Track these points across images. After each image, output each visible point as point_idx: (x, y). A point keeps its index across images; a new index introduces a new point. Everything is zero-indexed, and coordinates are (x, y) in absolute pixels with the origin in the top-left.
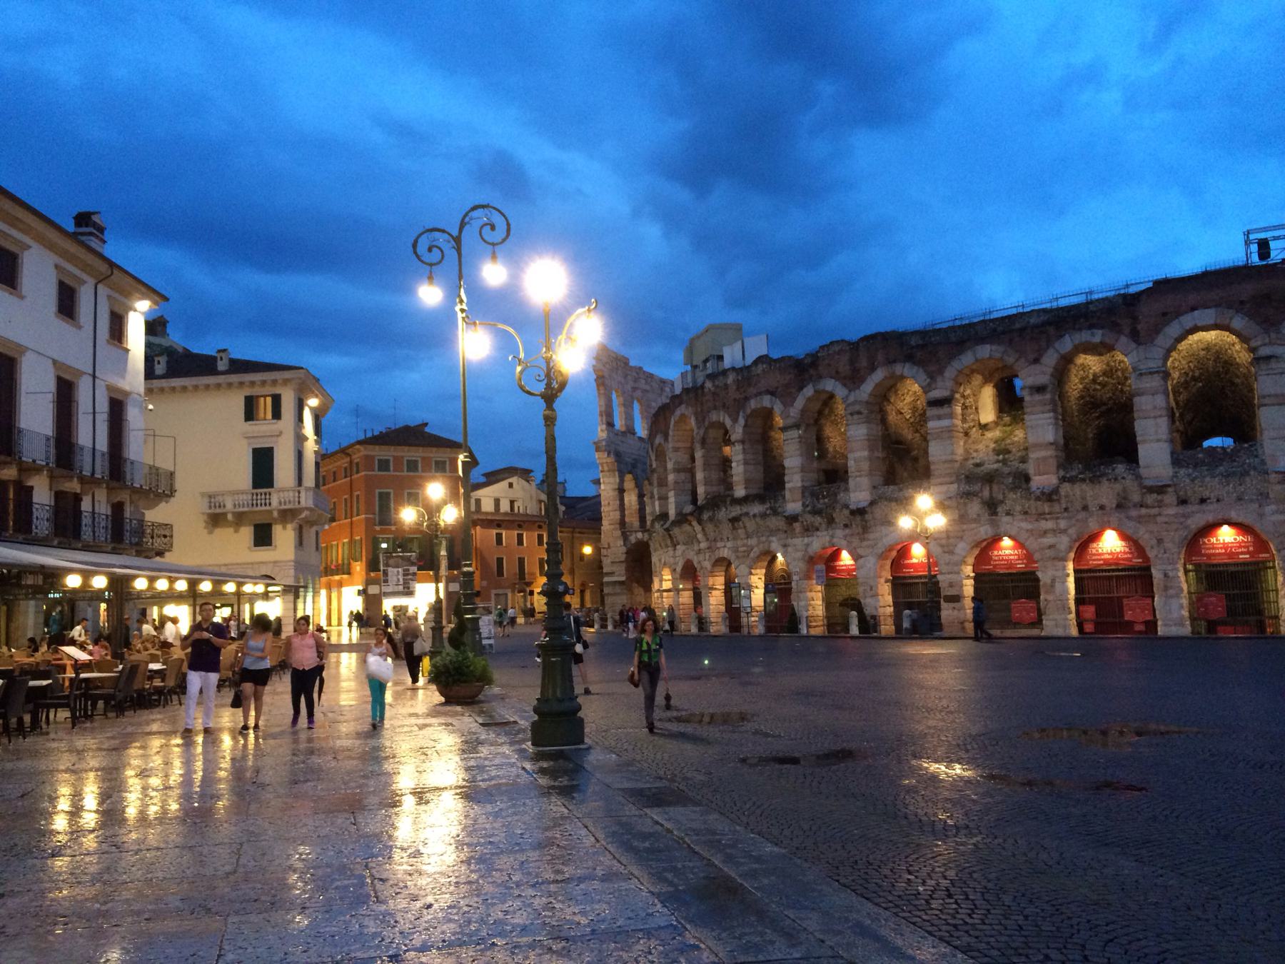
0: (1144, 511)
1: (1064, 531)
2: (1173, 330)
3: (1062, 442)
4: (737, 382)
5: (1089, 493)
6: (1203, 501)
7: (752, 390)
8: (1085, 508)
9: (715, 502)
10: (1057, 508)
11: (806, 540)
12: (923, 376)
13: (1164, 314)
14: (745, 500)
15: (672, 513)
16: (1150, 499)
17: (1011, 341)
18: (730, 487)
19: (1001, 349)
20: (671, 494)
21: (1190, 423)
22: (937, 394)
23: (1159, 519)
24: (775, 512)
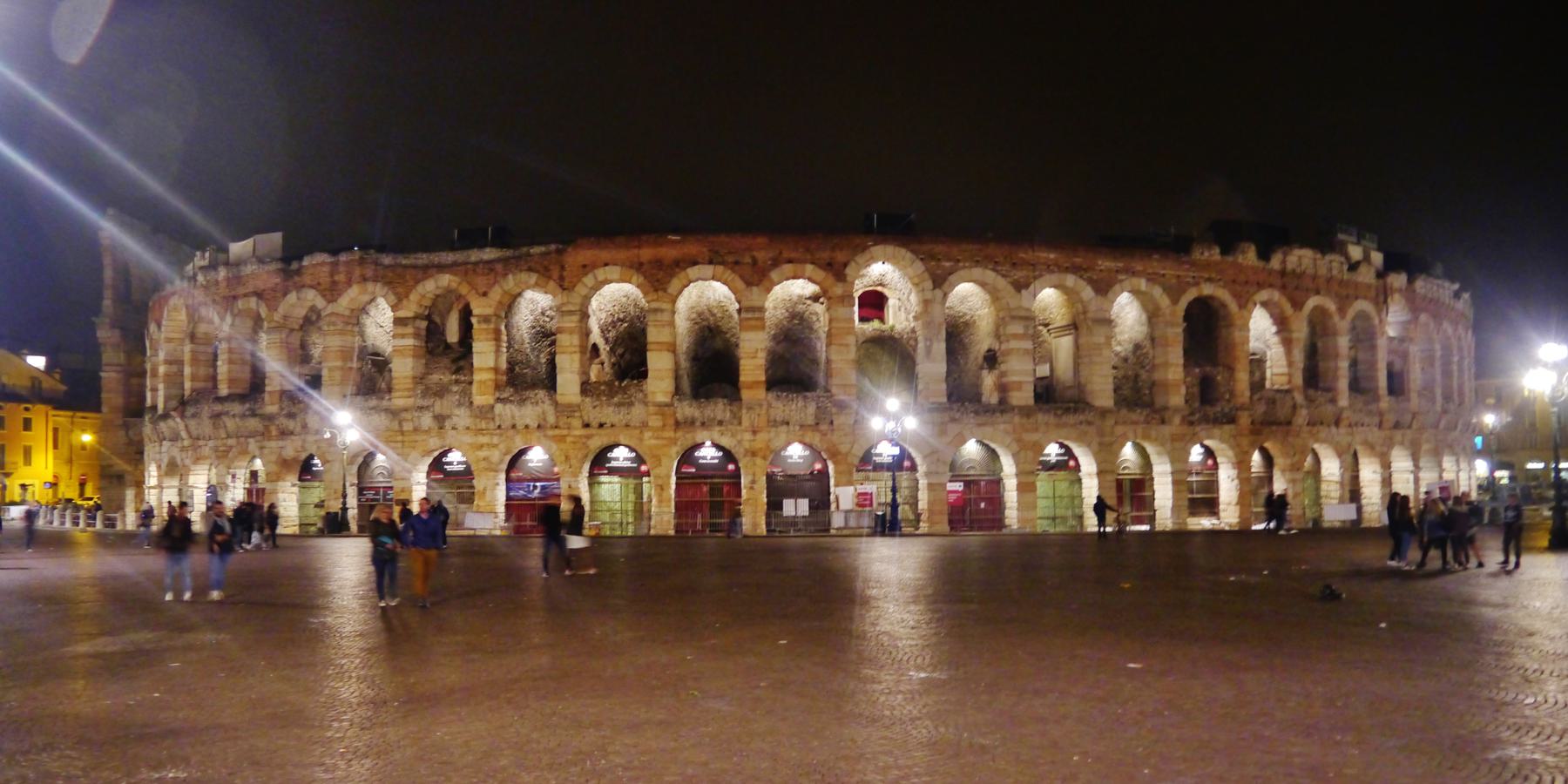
0: (557, 432)
1: (495, 446)
2: (589, 280)
3: (504, 366)
4: (228, 279)
5: (517, 414)
6: (601, 425)
7: (241, 290)
8: (514, 426)
9: (199, 396)
10: (492, 426)
11: (281, 443)
12: (392, 298)
13: (584, 266)
14: (230, 398)
15: (161, 406)
16: (562, 421)
17: (466, 273)
18: (215, 387)
19: (457, 279)
20: (161, 386)
21: (622, 356)
22: (401, 314)
23: (569, 439)
24: (254, 415)
